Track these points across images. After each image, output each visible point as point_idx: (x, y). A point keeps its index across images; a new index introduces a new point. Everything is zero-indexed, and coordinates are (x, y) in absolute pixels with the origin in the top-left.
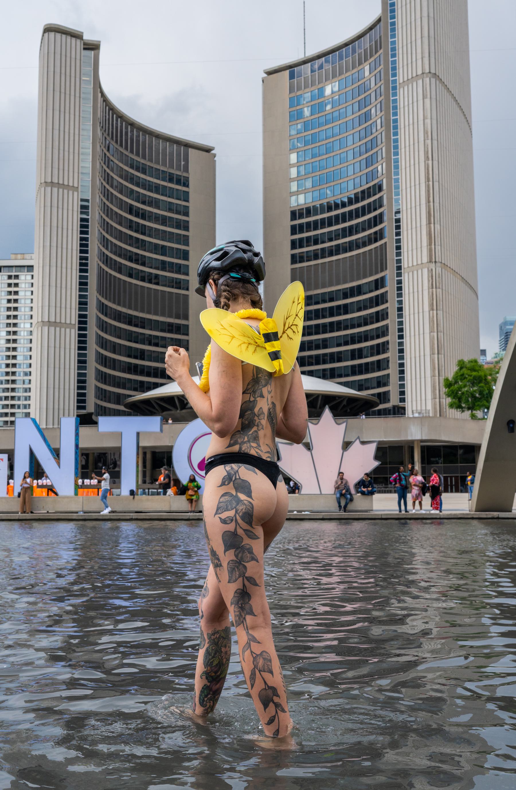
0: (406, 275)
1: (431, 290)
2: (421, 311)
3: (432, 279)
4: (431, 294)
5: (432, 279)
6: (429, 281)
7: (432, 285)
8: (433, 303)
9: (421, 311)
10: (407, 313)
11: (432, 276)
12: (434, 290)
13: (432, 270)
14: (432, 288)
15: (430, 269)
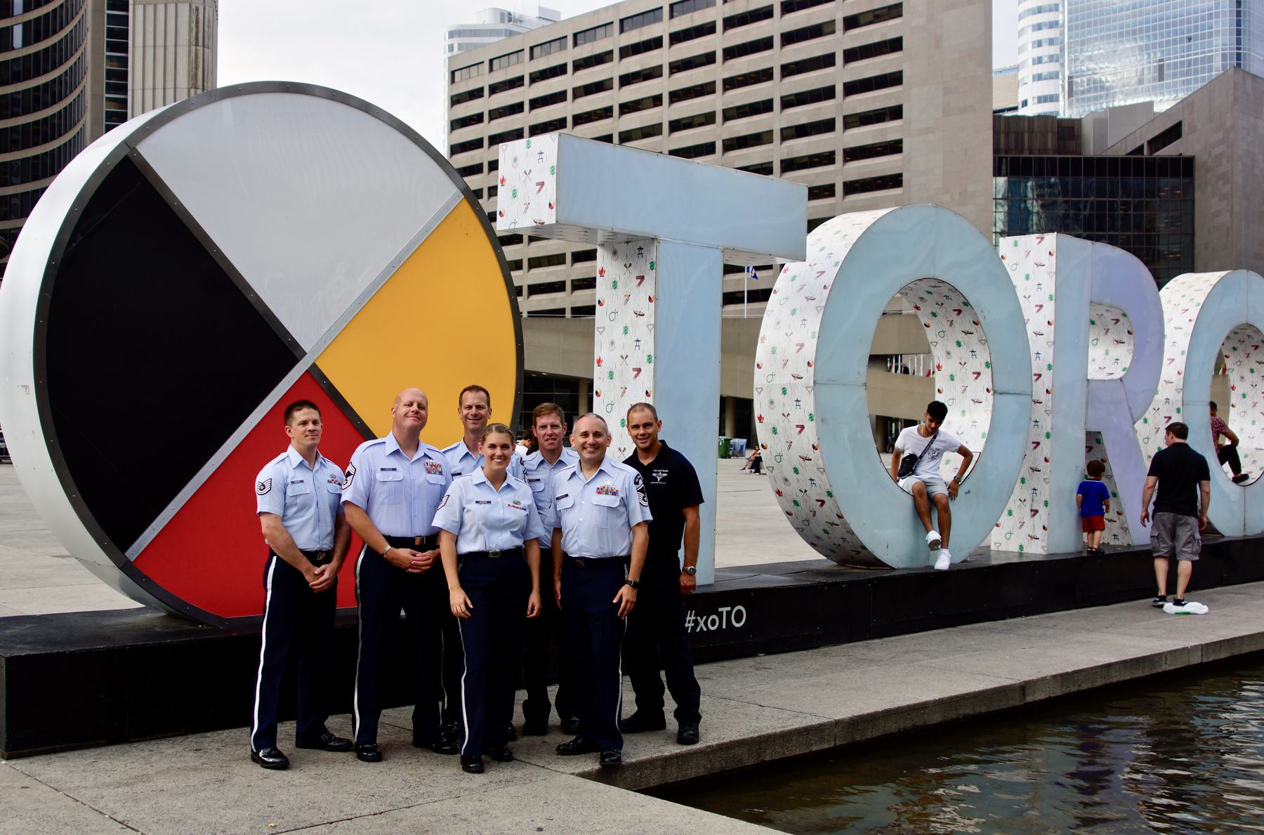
0: (140, 9)
1: (193, 48)
2: (170, 85)
3: (197, 27)
4: (193, 55)
5: (197, 27)
6: (190, 29)
7: (197, 38)
8: (196, 75)
9: (170, 85)
10: (138, 85)
11: (197, 22)
12: (200, 49)
13: (197, 9)
14: (197, 45)
15: (194, 7)
